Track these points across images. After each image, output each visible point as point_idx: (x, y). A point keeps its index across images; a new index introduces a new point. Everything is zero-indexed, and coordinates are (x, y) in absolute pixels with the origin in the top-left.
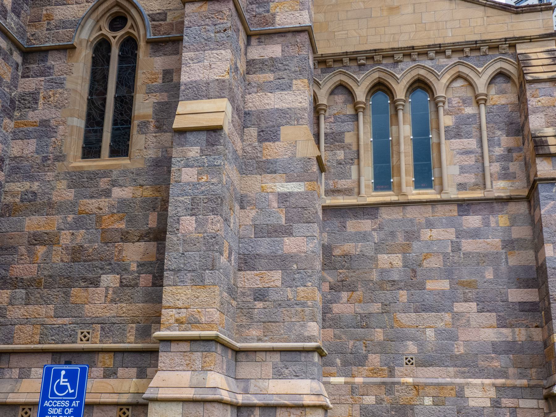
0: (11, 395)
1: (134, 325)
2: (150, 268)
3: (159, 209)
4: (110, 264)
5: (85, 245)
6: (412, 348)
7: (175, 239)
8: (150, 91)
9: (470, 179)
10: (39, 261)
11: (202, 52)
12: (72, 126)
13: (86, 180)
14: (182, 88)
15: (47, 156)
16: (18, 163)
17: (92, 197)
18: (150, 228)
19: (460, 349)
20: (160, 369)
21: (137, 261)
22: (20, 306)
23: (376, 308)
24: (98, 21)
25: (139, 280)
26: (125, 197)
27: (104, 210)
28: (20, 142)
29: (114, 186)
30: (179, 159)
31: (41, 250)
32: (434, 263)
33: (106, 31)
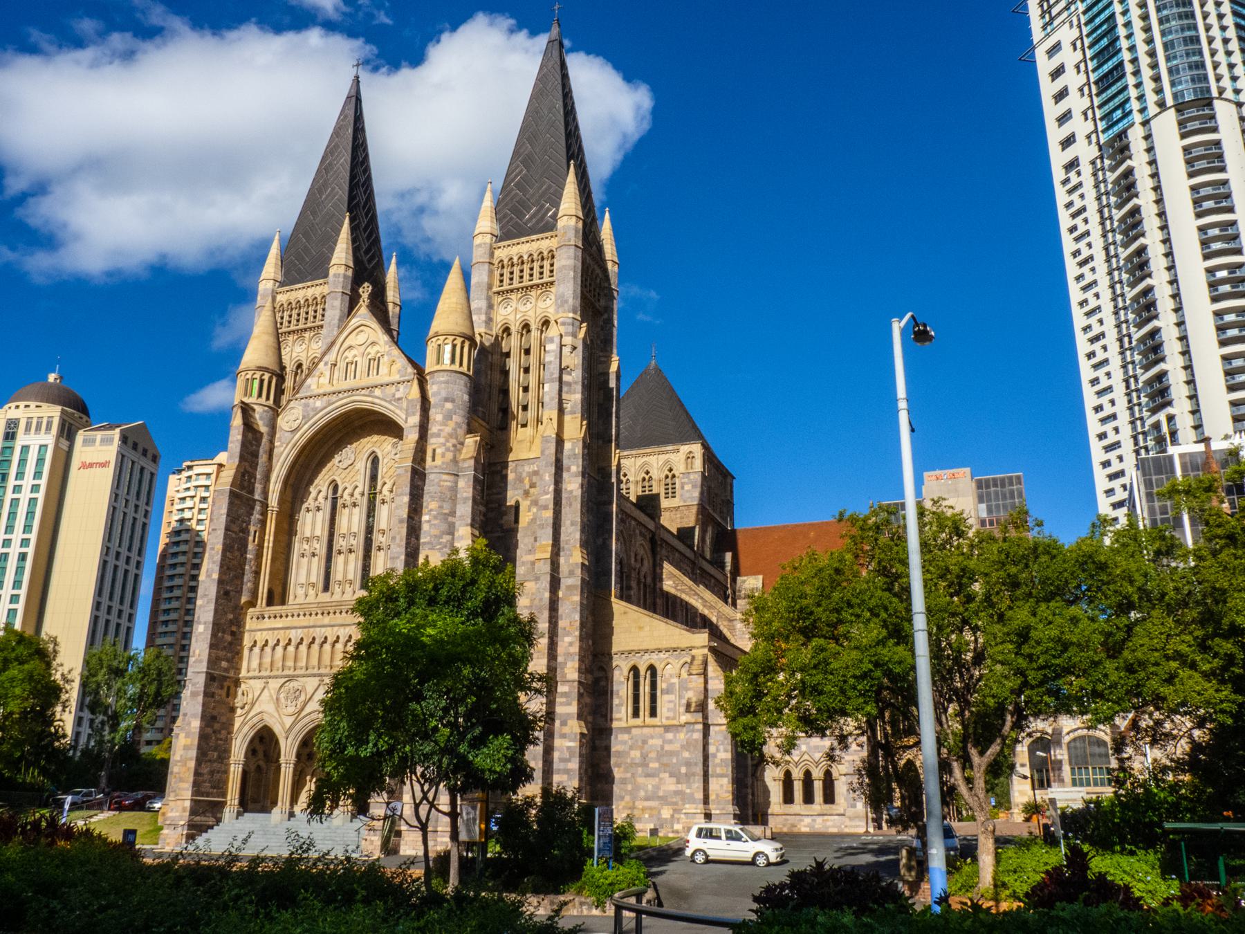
6: (642, 793)
9: (671, 714)
19: (661, 794)
23: (629, 775)
32: (653, 755)
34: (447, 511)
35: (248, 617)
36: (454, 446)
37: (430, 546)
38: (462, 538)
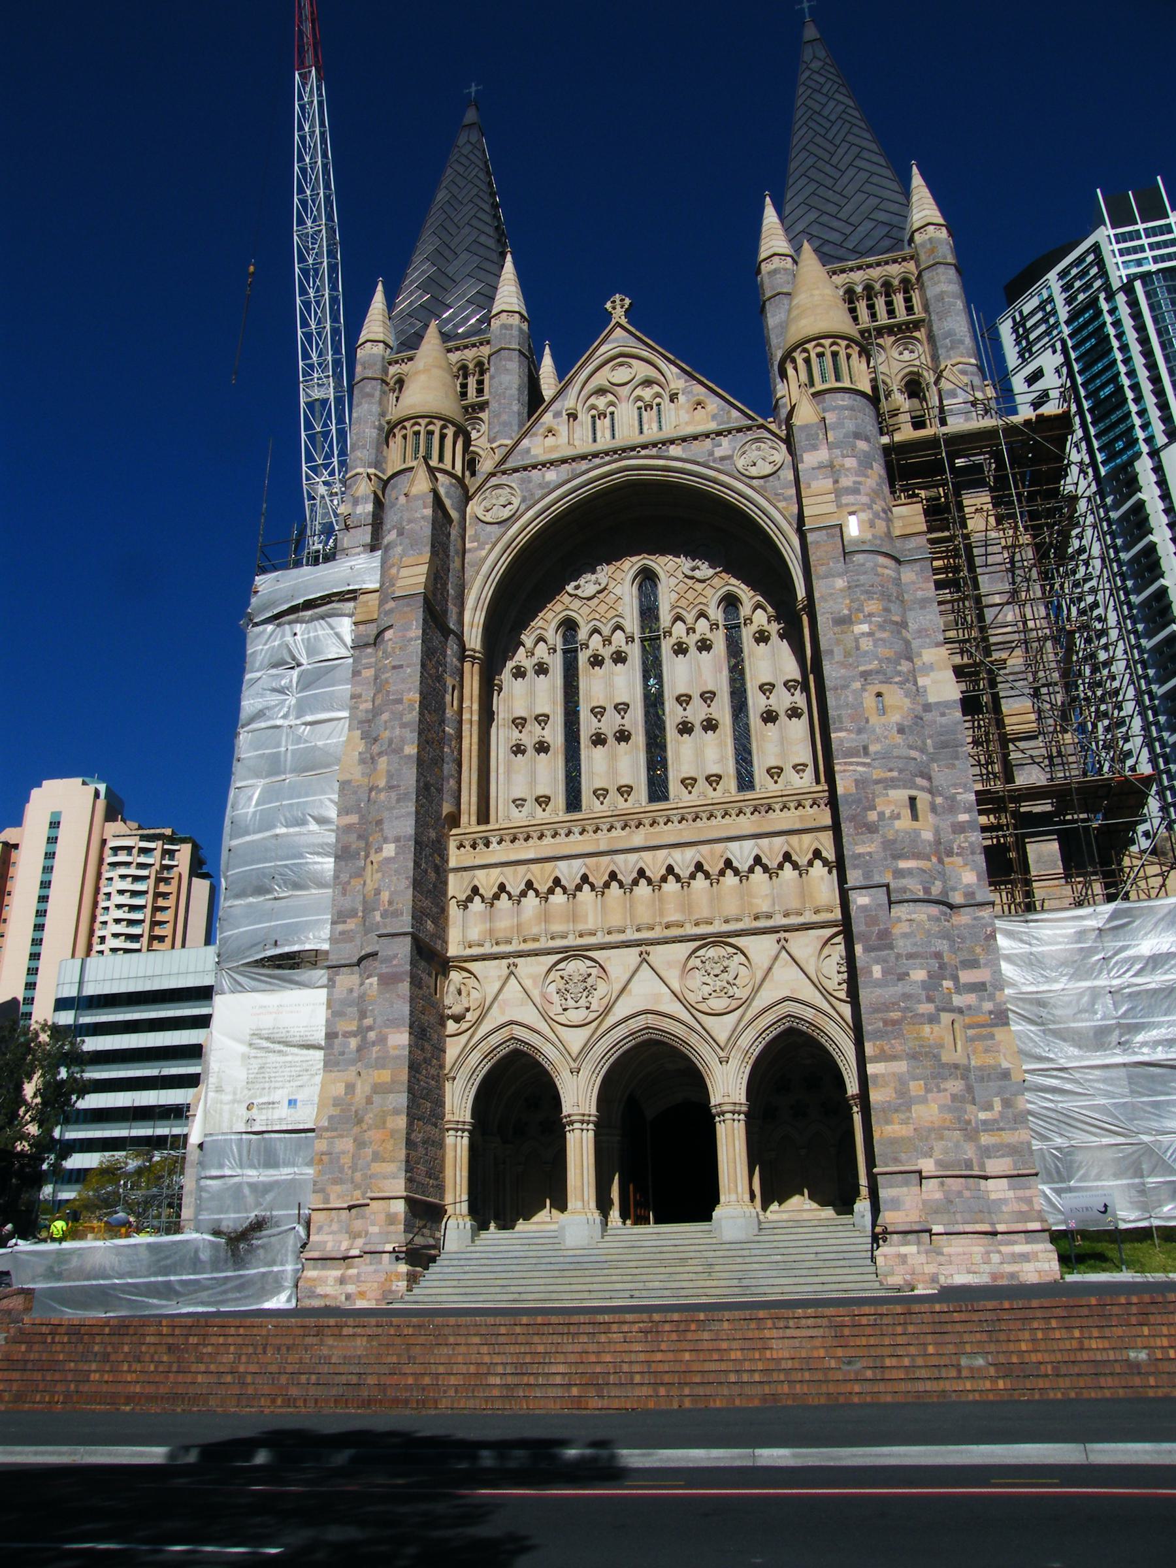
34: (897, 618)
35: (452, 845)
36: (884, 511)
37: (881, 677)
38: (929, 668)
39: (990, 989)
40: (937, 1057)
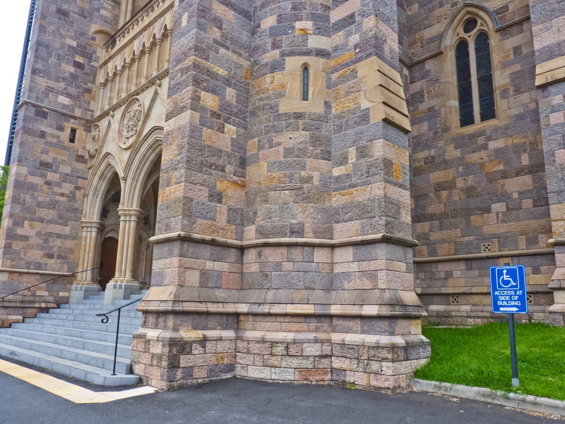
0: (443, 289)
1: (524, 237)
2: (530, 194)
3: (529, 151)
4: (497, 196)
5: (475, 186)
7: (553, 168)
8: (505, 65)
10: (444, 201)
11: (549, 22)
12: (450, 107)
13: (467, 141)
14: (537, 54)
15: (437, 131)
16: (418, 140)
17: (474, 152)
18: (524, 166)
20: (558, 266)
21: (518, 191)
22: (437, 232)
24: (455, 29)
25: (522, 204)
26: (499, 147)
27: (484, 159)
28: (417, 126)
29: (489, 141)
30: (545, 108)
31: (444, 194)
33: (463, 34)
39: (358, 18)
40: (274, 108)
